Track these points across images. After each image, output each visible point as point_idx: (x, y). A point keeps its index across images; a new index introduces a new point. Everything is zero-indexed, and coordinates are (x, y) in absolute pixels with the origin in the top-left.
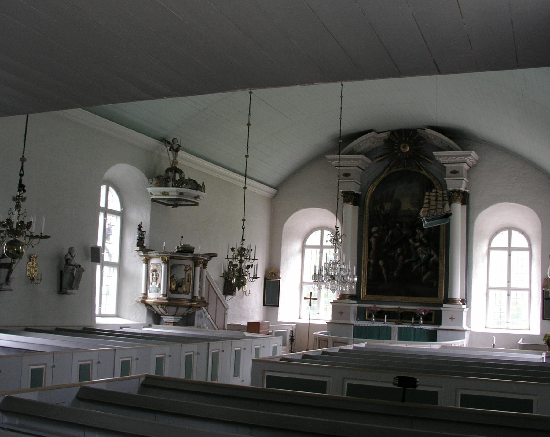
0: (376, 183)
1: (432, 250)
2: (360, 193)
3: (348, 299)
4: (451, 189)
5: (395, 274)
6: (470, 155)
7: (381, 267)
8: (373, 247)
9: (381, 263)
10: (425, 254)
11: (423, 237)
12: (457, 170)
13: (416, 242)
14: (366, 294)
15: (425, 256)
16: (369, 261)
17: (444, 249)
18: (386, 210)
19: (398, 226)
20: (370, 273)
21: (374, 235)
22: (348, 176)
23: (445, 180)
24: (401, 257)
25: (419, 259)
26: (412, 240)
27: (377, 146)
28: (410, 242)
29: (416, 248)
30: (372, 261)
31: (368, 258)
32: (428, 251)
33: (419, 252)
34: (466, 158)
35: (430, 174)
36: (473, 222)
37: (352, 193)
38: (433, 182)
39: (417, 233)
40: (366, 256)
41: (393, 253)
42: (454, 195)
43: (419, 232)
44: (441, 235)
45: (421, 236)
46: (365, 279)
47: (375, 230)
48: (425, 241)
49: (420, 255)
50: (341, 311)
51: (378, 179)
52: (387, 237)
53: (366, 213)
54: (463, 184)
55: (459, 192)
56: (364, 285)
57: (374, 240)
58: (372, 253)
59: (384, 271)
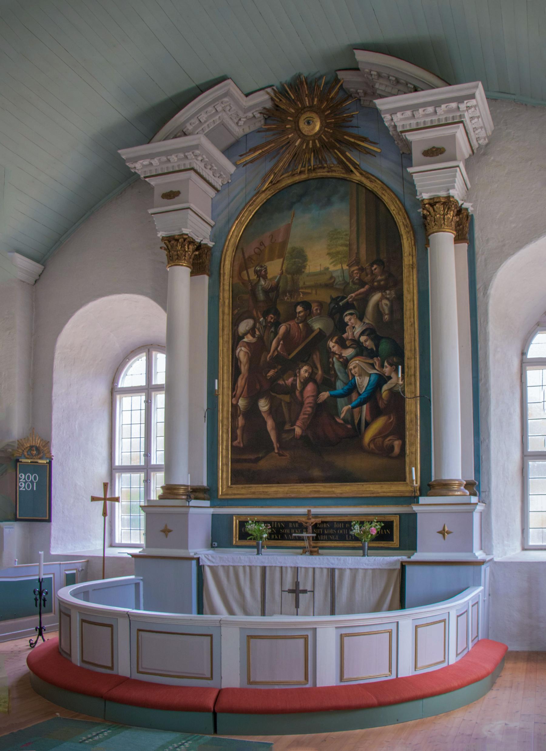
0: (247, 217)
1: (386, 364)
2: (211, 244)
3: (184, 497)
4: (426, 196)
5: (298, 431)
6: (472, 97)
7: (265, 415)
8: (244, 368)
9: (263, 405)
10: (370, 375)
11: (362, 334)
12: (438, 145)
14: (230, 484)
15: (369, 381)
16: (234, 402)
17: (415, 358)
18: (269, 276)
19: (299, 312)
20: (239, 432)
21: (245, 340)
22: (174, 197)
23: (411, 175)
24: (310, 387)
25: (353, 388)
26: (336, 342)
27: (247, 131)
28: (330, 349)
29: (345, 363)
30: (242, 403)
31: (233, 397)
32: (377, 367)
33: (353, 372)
34: (463, 106)
35: (373, 178)
36: (486, 288)
37: (185, 240)
38: (383, 196)
40: (228, 392)
41: (291, 380)
42: (434, 210)
43: (352, 321)
45: (358, 330)
46: (227, 446)
47: (247, 328)
48: (369, 344)
49: (357, 378)
50: (166, 526)
51: (250, 206)
53: (223, 289)
54: (456, 179)
55: (448, 202)
56: (224, 462)
57: (246, 352)
58: (241, 382)
59: (270, 424)
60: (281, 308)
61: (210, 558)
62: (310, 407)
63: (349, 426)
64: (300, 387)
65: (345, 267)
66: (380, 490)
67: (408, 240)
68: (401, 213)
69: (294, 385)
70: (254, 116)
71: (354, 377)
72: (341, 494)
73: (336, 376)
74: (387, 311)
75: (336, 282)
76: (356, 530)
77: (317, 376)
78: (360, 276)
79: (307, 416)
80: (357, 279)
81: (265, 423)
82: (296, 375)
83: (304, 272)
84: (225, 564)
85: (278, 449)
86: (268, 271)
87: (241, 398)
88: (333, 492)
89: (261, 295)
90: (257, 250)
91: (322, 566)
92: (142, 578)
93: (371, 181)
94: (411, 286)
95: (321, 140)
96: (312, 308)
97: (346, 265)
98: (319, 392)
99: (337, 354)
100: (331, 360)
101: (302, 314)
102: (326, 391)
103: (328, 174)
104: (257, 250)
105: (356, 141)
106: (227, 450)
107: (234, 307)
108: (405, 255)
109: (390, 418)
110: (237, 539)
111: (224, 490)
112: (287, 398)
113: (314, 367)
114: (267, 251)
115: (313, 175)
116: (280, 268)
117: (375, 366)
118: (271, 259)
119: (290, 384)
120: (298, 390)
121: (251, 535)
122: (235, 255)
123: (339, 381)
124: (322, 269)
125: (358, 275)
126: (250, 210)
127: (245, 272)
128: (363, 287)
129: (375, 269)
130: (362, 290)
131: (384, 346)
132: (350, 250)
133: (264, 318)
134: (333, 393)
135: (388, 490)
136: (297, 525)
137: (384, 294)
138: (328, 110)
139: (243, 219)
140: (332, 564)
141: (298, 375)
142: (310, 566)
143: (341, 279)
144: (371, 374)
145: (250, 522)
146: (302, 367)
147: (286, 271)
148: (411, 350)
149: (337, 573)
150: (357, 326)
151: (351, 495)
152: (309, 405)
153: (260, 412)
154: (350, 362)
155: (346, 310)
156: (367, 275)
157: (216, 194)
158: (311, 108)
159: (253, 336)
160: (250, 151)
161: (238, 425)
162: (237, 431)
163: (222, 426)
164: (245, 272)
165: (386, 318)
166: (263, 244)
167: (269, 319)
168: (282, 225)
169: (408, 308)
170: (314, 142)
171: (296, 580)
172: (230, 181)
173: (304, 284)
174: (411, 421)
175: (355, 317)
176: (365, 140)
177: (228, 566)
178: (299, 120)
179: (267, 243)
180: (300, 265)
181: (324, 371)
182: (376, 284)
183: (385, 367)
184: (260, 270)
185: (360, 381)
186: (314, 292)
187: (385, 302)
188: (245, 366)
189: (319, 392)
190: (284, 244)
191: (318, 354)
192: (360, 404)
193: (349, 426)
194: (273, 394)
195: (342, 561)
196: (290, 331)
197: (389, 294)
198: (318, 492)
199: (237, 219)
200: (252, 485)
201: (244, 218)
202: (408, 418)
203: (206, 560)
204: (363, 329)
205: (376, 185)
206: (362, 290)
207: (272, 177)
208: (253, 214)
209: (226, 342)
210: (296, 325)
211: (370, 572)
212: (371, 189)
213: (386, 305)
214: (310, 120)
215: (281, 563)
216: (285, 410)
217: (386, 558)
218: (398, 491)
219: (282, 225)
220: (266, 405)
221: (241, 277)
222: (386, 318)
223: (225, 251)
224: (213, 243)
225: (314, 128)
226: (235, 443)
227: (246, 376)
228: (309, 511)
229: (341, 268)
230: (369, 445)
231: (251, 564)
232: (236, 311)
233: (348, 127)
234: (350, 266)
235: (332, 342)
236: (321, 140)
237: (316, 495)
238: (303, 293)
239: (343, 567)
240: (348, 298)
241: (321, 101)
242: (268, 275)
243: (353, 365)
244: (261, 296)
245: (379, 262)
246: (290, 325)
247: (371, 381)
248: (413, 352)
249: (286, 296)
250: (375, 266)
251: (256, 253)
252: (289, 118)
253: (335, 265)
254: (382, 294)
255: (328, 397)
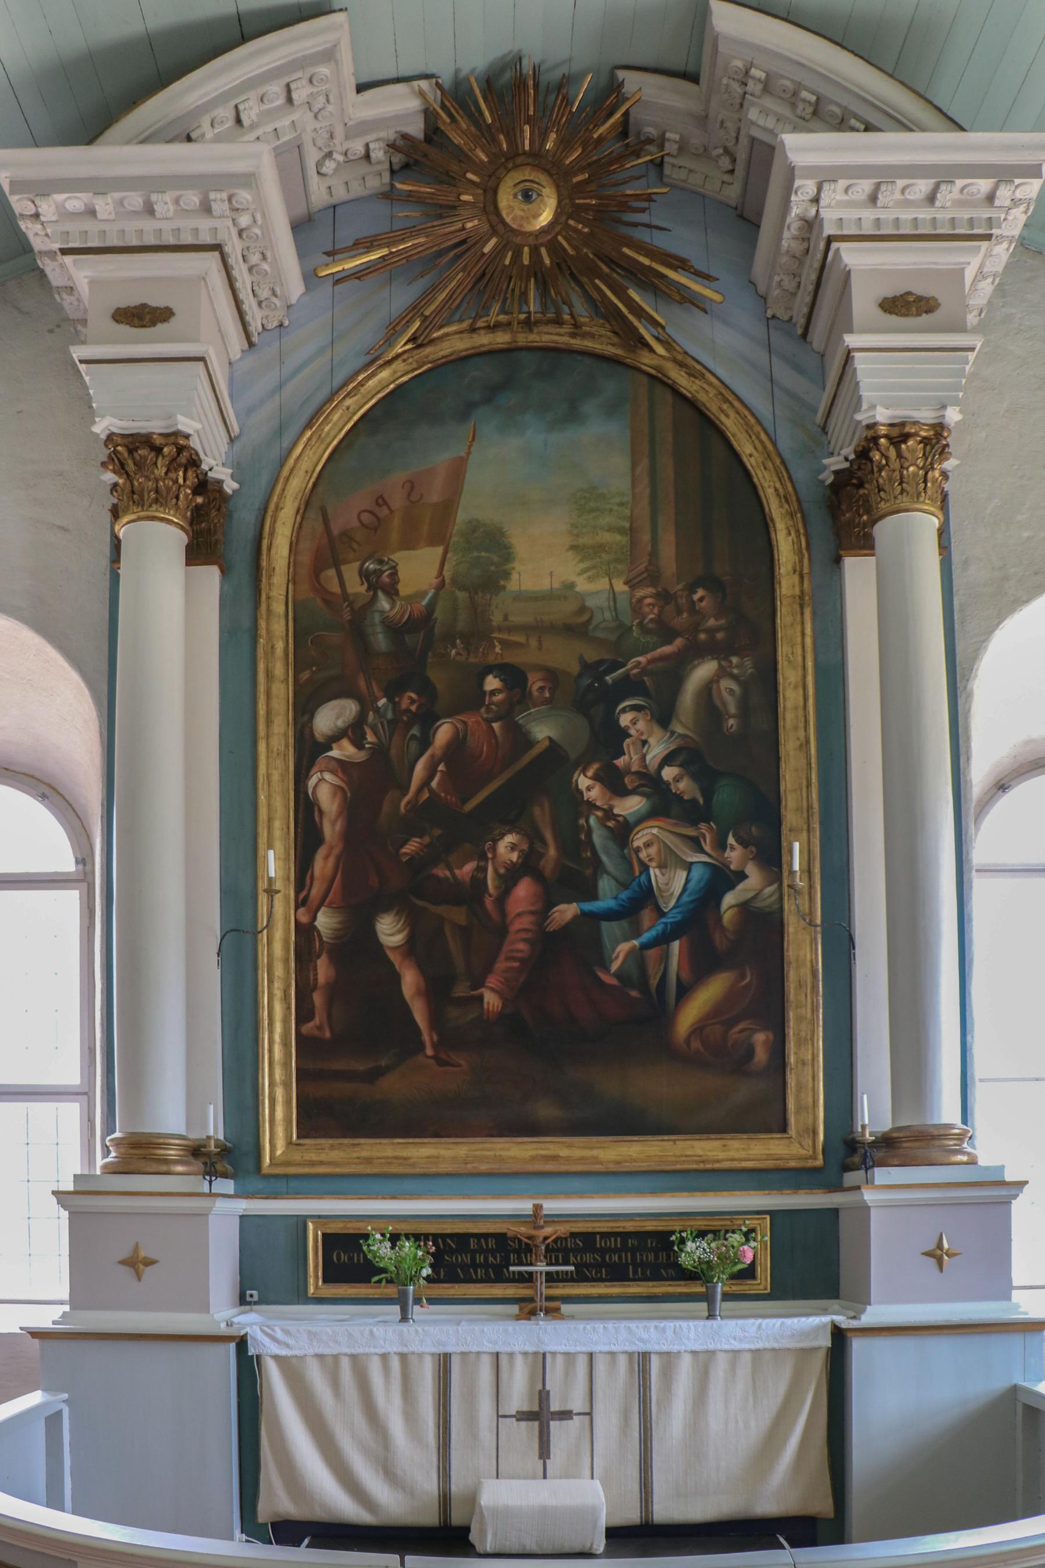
1: (731, 840)
2: (230, 486)
5: (491, 1000)
7: (394, 958)
8: (331, 829)
10: (689, 867)
11: (668, 760)
13: (622, 792)
15: (687, 881)
16: (304, 919)
19: (493, 693)
20: (318, 999)
21: (335, 753)
24: (524, 890)
26: (596, 778)
28: (581, 793)
30: (325, 922)
32: (707, 848)
33: (643, 855)
35: (698, 367)
38: (723, 418)
39: (625, 734)
40: (286, 891)
41: (469, 867)
43: (641, 725)
44: (789, 746)
45: (657, 749)
47: (340, 723)
48: (685, 787)
49: (654, 872)
52: (420, 768)
53: (269, 610)
58: (322, 865)
59: (410, 981)
60: (437, 676)
61: (279, 1335)
62: (525, 940)
63: (634, 993)
64: (496, 888)
65: (620, 586)
66: (722, 1155)
67: (789, 534)
68: (770, 465)
69: (478, 882)
70: (367, 156)
71: (645, 868)
72: (618, 1163)
73: (597, 863)
74: (732, 709)
75: (594, 624)
76: (693, 1252)
77: (542, 863)
78: (660, 612)
79: (516, 964)
80: (652, 620)
81: (397, 979)
82: (486, 854)
83: (504, 588)
84: (327, 1351)
85: (435, 1046)
86: (401, 575)
87: (323, 909)
88: (596, 1160)
89: (381, 637)
90: (366, 518)
91: (614, 1348)
92: (66, 1396)
93: (690, 375)
94: (799, 650)
95: (554, 248)
96: (529, 685)
97: (621, 582)
98: (548, 903)
99: (598, 808)
100: (582, 821)
101: (499, 697)
102: (569, 902)
103: (573, 341)
104: (366, 518)
105: (655, 265)
106: (286, 1044)
107: (300, 662)
108: (783, 570)
109: (743, 977)
110: (320, 1283)
111: (279, 1152)
112: (458, 915)
113: (534, 836)
114: (396, 522)
115: (523, 339)
116: (434, 572)
117: (703, 843)
118: (408, 543)
119: (467, 879)
120: (490, 896)
121: (384, 1270)
122: (301, 524)
123: (605, 876)
124: (556, 585)
125: (656, 610)
126: (348, 408)
127: (331, 572)
128: (669, 641)
129: (701, 599)
130: (667, 649)
131: (726, 795)
132: (633, 543)
133: (391, 700)
134: (589, 906)
135: (742, 1154)
136: (492, 1243)
137: (723, 663)
138: (582, 170)
139: (327, 428)
140: (641, 1340)
141: (490, 855)
142: (579, 1349)
143: (607, 615)
144: (692, 863)
145: (378, 1236)
146: (502, 836)
147: (454, 581)
148: (799, 809)
149: (655, 1364)
150: (652, 741)
151: (644, 1166)
152: (524, 935)
153: (380, 946)
154: (636, 830)
155: (623, 700)
156: (679, 612)
157: (243, 351)
158: (537, 159)
159: (359, 744)
160: (357, 244)
161: (316, 979)
162: (312, 997)
163: (271, 981)
164: (331, 572)
165: (732, 726)
166: (385, 503)
167: (405, 704)
168: (442, 458)
169: (789, 705)
170: (535, 251)
171: (540, 1387)
172: (286, 323)
173: (506, 618)
174: (800, 985)
175: (649, 718)
176: (681, 264)
177: (336, 1357)
178: (498, 185)
179: (397, 501)
180: (493, 568)
181: (561, 848)
182: (702, 636)
183: (728, 849)
184: (375, 571)
185: (662, 880)
186: (533, 642)
187: (726, 684)
188: (333, 823)
189: (548, 903)
190: (448, 507)
191: (546, 805)
192: (664, 940)
193: (634, 993)
194: (420, 903)
195: (670, 1333)
196: (465, 738)
197: (737, 667)
198: (555, 1158)
199: (309, 425)
200: (362, 1141)
201: (330, 425)
202: (792, 977)
203: (266, 1341)
204: (671, 749)
205: (705, 386)
206: (667, 649)
207: (417, 324)
208: (356, 418)
209: (278, 754)
210: (484, 725)
211: (747, 1358)
212: (689, 395)
213: (731, 692)
214: (531, 190)
215: (496, 1343)
216: (454, 945)
217: (789, 1321)
218: (769, 1157)
219: (442, 458)
220: (399, 932)
221: (320, 584)
222: (730, 724)
223: (272, 506)
224: (236, 486)
225: (536, 216)
226: (308, 1028)
227: (336, 851)
228: (538, 1208)
229: (608, 587)
230: (688, 1041)
231: (405, 1350)
232: (305, 675)
233: (636, 225)
234: (632, 584)
235: (586, 776)
236: (554, 248)
237: (549, 1167)
238: (500, 641)
239: (675, 1348)
240: (628, 667)
241: (565, 144)
242: (400, 587)
243: (645, 839)
244: (381, 641)
245: (710, 582)
246: (464, 723)
247: (692, 885)
248: (805, 815)
249: (454, 646)
250: (700, 593)
251: (363, 525)
252: (470, 176)
253: (590, 579)
254: (720, 664)
255: (575, 918)
